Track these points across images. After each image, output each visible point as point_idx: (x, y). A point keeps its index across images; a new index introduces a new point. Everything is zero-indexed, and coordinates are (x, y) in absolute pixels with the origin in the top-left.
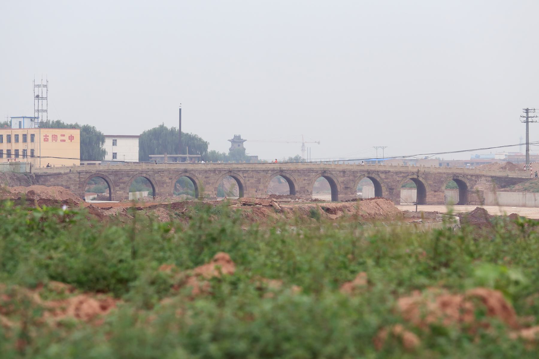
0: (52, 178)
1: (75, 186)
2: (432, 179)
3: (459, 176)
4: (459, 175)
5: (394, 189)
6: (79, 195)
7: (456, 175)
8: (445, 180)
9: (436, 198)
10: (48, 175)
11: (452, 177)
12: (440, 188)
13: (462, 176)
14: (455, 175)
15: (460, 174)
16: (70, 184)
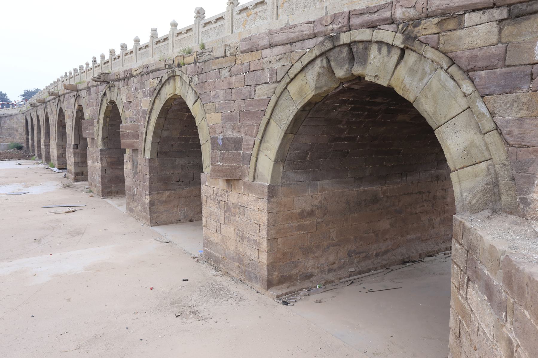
0: (8, 120)
1: (21, 129)
2: (221, 93)
3: (367, 43)
4: (364, 35)
5: (138, 149)
6: (23, 139)
7: (345, 38)
8: (274, 99)
9: (229, 231)
10: (6, 117)
11: (318, 61)
12: (247, 159)
13: (399, 41)
14: (333, 38)
15: (373, 26)
16: (18, 127)
